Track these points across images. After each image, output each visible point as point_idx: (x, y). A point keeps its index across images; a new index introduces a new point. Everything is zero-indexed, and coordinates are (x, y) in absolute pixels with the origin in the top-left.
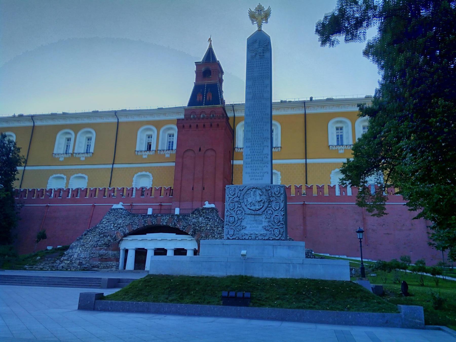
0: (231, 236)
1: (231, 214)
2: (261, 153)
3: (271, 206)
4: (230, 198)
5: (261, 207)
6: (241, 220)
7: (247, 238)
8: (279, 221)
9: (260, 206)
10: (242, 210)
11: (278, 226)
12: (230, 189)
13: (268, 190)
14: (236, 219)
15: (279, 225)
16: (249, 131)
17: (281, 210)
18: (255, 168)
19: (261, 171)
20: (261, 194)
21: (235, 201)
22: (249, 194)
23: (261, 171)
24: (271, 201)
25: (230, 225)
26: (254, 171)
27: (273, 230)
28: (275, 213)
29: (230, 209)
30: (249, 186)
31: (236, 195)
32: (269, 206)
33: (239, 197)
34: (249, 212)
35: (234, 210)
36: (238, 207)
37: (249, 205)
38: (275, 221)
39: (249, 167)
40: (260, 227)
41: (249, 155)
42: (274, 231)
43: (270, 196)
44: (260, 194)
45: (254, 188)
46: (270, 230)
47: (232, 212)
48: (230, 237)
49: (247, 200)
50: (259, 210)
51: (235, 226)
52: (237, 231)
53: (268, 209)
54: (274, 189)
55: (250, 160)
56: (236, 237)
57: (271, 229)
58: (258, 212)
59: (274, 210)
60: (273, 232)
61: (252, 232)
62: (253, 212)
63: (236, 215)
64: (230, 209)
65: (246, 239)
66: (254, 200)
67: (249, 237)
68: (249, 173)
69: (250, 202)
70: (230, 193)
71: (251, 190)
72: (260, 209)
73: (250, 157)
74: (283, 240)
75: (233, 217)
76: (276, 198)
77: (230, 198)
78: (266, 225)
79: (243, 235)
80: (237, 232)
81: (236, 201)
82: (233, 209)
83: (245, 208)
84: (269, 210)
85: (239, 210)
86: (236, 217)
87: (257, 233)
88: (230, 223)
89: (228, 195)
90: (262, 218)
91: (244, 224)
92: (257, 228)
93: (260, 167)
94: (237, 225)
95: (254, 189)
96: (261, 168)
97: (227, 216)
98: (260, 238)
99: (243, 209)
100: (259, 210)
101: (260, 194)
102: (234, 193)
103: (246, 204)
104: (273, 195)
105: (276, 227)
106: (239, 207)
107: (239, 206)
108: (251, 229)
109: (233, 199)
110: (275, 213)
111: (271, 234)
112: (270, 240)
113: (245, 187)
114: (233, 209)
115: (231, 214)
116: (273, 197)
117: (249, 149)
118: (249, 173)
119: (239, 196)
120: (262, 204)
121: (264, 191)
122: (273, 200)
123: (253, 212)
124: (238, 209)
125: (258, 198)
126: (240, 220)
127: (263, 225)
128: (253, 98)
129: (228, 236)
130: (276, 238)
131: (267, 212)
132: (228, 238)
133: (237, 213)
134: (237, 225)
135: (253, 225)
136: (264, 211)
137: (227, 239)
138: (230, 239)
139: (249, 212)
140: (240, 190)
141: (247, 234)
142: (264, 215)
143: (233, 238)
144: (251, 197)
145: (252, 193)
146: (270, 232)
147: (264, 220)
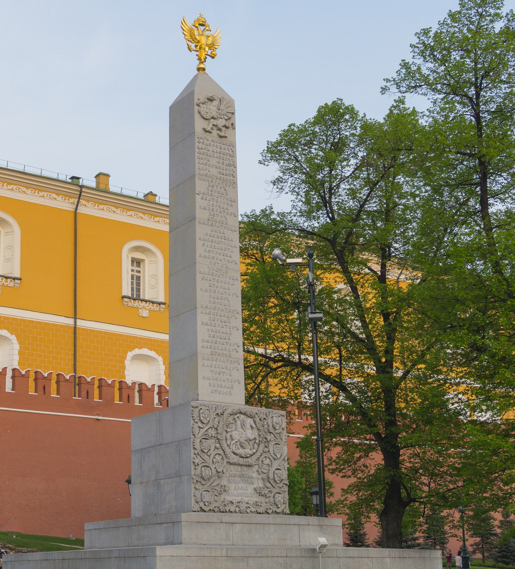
0: (207, 504)
1: (204, 461)
2: (226, 341)
3: (269, 451)
4: (201, 430)
5: (254, 451)
6: (219, 474)
7: (232, 509)
8: (282, 480)
9: (254, 448)
10: (223, 455)
11: (281, 488)
12: (201, 411)
13: (262, 419)
14: (214, 471)
15: (281, 486)
16: (206, 291)
17: (284, 460)
18: (218, 370)
19: (228, 377)
20: (254, 426)
21: (211, 435)
22: (233, 423)
23: (228, 377)
24: (268, 441)
25: (203, 482)
26: (217, 375)
27: (272, 495)
28: (276, 465)
29: (202, 450)
30: (232, 408)
31: (210, 425)
32: (266, 450)
33: (216, 429)
34: (235, 459)
35: (209, 454)
36: (216, 448)
37: (234, 446)
38: (276, 480)
39: (208, 366)
40: (250, 489)
41: (207, 342)
42: (274, 497)
43: (266, 430)
44: (251, 426)
45: (241, 413)
46: (268, 496)
47: (206, 457)
48: (204, 508)
49: (231, 436)
50: (251, 456)
51: (212, 485)
52: (216, 495)
53: (264, 455)
54: (272, 417)
55: (209, 351)
56: (215, 507)
57: (269, 494)
58: (250, 461)
59: (274, 458)
60: (272, 499)
61: (239, 499)
62: (241, 461)
63: (213, 463)
64: (202, 450)
65: (231, 512)
66: (244, 435)
67: (236, 506)
68: (209, 379)
69: (236, 441)
70: (202, 419)
71: (238, 417)
72: (252, 455)
73: (209, 345)
74: (288, 514)
75: (209, 467)
76: (275, 436)
77: (200, 427)
78: (261, 485)
79: (226, 504)
80: (216, 497)
81: (212, 436)
82: (208, 452)
83: (228, 451)
84: (266, 457)
85: (218, 454)
86: (213, 467)
87: (246, 499)
88: (203, 479)
89: (197, 422)
90: (253, 473)
91: (224, 482)
92: (245, 492)
93: (226, 368)
94: (214, 484)
95: (242, 416)
96: (228, 371)
97: (198, 465)
98: (253, 510)
99: (224, 452)
100: (251, 456)
101: (251, 426)
102: (208, 419)
103: (228, 442)
104: (272, 430)
105: (278, 490)
106: (218, 449)
107: (218, 445)
108: (235, 492)
109: (206, 431)
110: (276, 465)
111: (270, 502)
112: (268, 513)
113: (225, 410)
114: (208, 452)
115: (204, 461)
116: (271, 433)
117: (207, 327)
118: (209, 379)
119: (216, 426)
120: (256, 446)
121: (257, 420)
122: (270, 440)
123: (241, 461)
124: (217, 451)
125: (251, 434)
126: (220, 474)
127: (255, 486)
128: (210, 223)
129: (202, 504)
130: (279, 510)
131: (262, 461)
132: (201, 508)
133: (215, 460)
134: (214, 484)
135: (240, 485)
136: (259, 458)
137: (199, 509)
138: (205, 511)
139: (235, 459)
140: (217, 414)
141: (232, 503)
142: (257, 466)
143: (210, 510)
144: (236, 429)
145: (239, 422)
146: (267, 500)
147: (255, 475)
